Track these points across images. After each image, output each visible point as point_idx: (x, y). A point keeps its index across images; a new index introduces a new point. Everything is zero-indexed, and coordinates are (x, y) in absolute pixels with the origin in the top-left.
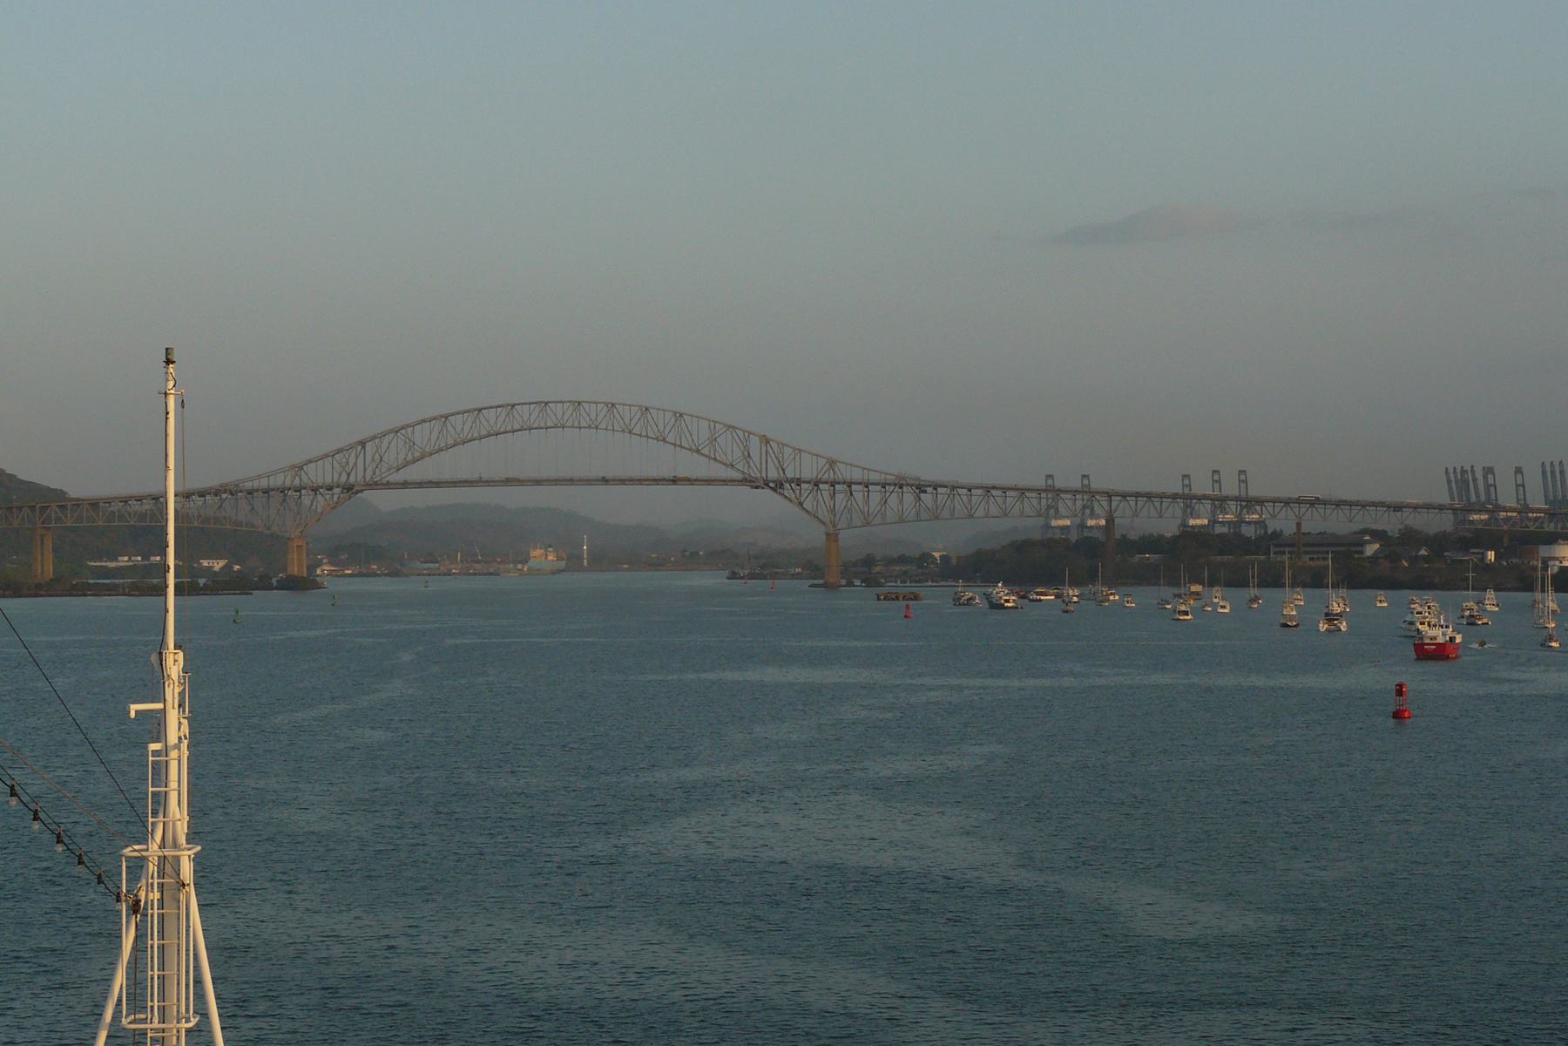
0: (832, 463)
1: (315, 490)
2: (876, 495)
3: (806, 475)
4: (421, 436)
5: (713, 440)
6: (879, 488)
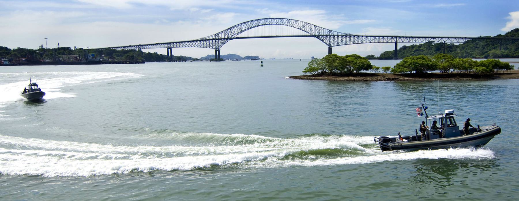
0: (330, 31)
1: (221, 39)
2: (340, 38)
3: (325, 34)
4: (243, 27)
5: (304, 26)
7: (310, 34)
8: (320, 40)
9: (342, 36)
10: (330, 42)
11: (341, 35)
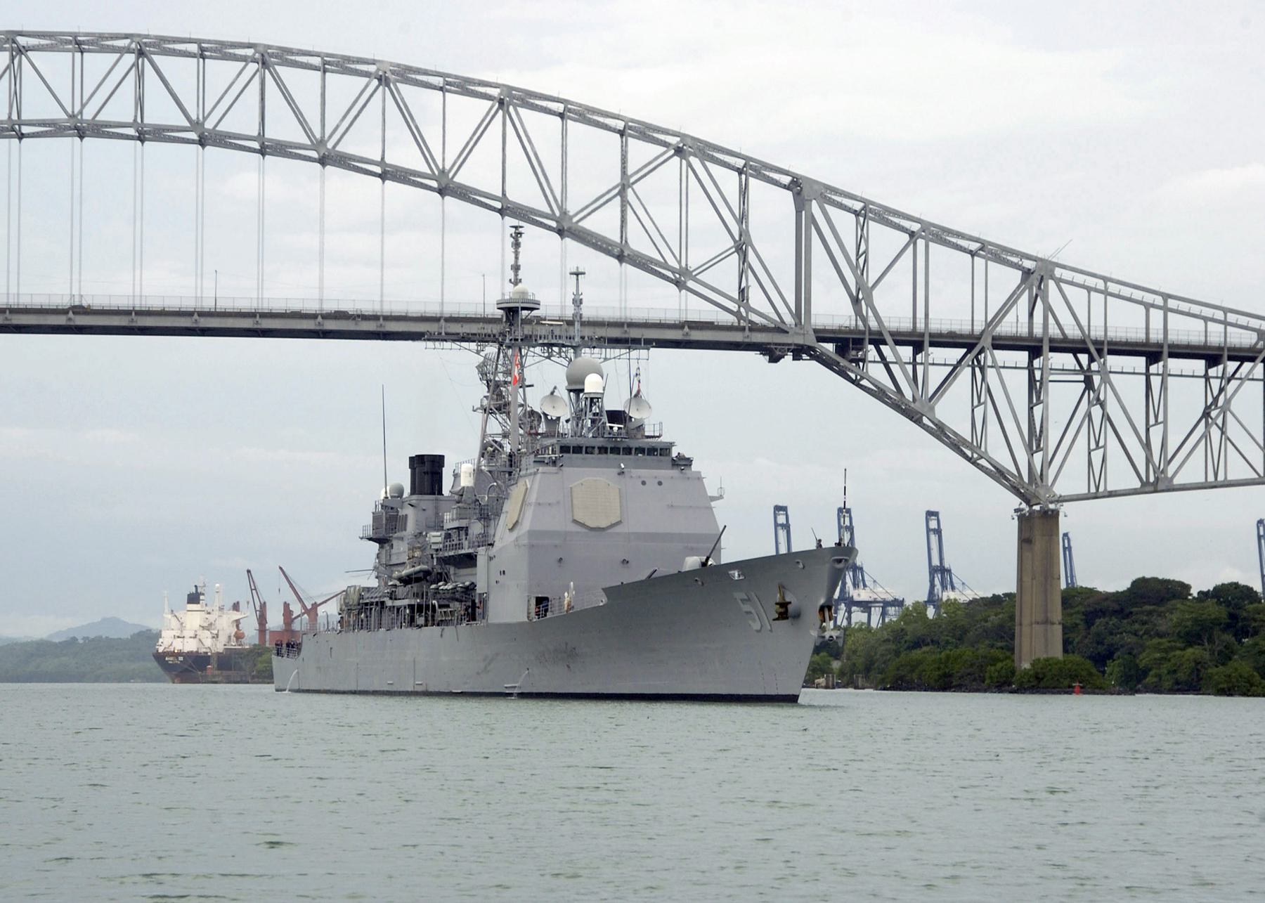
6: (1199, 364)
7: (737, 314)
8: (879, 393)
9: (1212, 357)
10: (1035, 439)
11: (1137, 335)
